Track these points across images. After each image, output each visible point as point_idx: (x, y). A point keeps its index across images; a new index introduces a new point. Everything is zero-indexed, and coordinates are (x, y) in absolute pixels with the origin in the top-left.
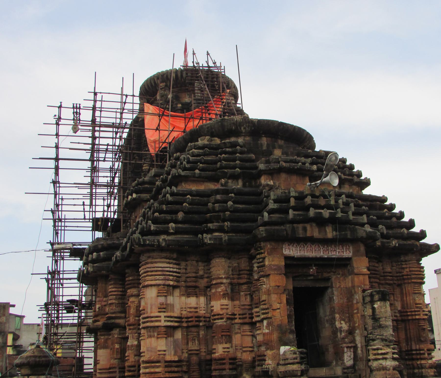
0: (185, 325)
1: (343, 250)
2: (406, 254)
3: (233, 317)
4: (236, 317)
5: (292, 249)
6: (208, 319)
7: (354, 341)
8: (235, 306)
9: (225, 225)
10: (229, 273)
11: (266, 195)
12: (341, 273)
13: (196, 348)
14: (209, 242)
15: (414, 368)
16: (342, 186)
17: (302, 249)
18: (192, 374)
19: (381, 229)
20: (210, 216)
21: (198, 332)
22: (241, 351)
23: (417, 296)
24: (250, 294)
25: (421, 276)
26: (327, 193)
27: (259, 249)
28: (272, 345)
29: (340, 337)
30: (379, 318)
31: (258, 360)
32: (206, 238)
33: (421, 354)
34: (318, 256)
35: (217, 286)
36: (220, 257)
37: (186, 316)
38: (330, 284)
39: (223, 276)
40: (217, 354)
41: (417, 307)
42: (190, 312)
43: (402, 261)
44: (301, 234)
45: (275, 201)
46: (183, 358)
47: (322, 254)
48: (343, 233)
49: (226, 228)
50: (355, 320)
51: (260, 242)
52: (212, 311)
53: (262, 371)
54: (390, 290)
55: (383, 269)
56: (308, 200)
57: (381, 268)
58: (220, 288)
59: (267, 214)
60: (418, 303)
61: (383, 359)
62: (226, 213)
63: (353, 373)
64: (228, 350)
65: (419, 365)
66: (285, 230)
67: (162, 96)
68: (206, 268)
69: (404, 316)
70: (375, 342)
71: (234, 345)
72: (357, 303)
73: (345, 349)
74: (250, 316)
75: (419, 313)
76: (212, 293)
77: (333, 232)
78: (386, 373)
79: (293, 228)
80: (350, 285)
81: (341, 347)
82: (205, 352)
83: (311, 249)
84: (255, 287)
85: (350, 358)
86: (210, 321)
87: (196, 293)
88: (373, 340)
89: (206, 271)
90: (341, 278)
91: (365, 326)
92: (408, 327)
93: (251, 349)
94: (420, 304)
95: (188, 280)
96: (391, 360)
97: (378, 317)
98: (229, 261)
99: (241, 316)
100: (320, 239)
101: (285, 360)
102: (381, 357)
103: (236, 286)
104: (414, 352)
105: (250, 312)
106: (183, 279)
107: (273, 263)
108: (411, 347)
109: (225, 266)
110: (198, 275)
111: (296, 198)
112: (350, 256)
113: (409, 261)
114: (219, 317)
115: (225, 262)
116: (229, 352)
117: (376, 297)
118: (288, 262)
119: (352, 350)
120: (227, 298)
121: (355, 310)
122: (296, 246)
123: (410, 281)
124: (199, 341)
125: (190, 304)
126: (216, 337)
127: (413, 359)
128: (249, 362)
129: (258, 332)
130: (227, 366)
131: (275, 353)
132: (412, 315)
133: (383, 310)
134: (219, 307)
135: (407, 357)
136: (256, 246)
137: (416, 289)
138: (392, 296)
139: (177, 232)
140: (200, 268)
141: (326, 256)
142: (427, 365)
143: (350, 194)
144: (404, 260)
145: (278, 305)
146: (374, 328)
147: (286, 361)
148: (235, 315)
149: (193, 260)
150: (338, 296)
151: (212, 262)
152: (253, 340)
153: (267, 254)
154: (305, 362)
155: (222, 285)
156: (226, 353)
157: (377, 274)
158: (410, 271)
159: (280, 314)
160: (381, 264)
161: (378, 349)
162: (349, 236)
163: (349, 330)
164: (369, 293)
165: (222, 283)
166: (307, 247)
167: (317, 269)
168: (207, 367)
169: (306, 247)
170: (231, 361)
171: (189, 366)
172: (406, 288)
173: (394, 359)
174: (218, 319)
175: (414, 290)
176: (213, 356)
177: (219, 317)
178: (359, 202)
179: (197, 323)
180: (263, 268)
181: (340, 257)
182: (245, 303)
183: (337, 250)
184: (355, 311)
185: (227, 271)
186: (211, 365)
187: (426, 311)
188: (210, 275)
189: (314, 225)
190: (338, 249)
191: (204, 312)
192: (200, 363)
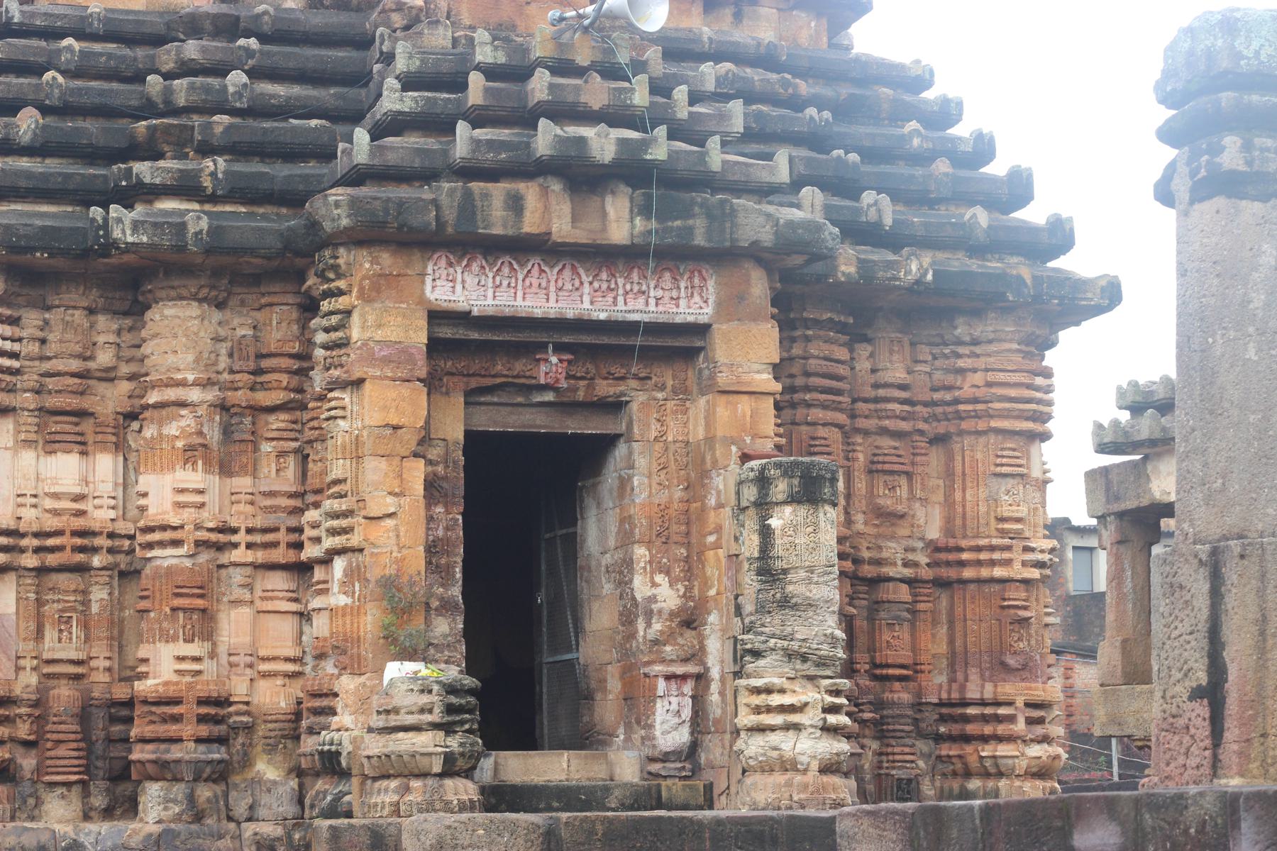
0: (30, 561)
1: (675, 294)
2: (976, 313)
3: (222, 538)
4: (235, 538)
5: (463, 282)
6: (127, 543)
7: (697, 655)
8: (234, 498)
9: (201, 170)
10: (215, 364)
11: (384, 49)
12: (670, 383)
13: (73, 655)
14: (130, 239)
15: (968, 774)
16: (747, 9)
17: (505, 283)
18: (52, 753)
19: (869, 206)
20: (148, 127)
21: (85, 592)
22: (248, 671)
23: (1009, 486)
24: (296, 451)
25: (1046, 409)
26: (623, 58)
27: (332, 275)
28: (359, 655)
29: (644, 637)
30: (785, 571)
31: (308, 709)
32: (119, 220)
33: (998, 719)
34: (570, 314)
35: (164, 412)
36: (182, 298)
37: (35, 528)
38: (624, 425)
39: (191, 377)
40: (150, 682)
41: (1003, 533)
42: (56, 513)
43: (960, 343)
44: (497, 222)
45: (409, 83)
46: (18, 691)
47: (587, 305)
48: (678, 223)
49: (207, 183)
50: (709, 571)
51: (336, 246)
52: (143, 509)
53: (321, 753)
54: (899, 456)
55: (874, 371)
56: (540, 86)
57: (867, 365)
58: (174, 424)
59: (367, 137)
60: (1006, 514)
61: (788, 727)
62: (216, 118)
63: (685, 778)
64: (196, 667)
65: (988, 763)
66: (435, 202)
68: (128, 338)
69: (948, 564)
70: (762, 662)
71: (222, 650)
72: (720, 506)
73: (661, 685)
74: (293, 537)
75: (1006, 555)
76: (145, 439)
77: (632, 220)
78: (789, 784)
79: (468, 195)
80: (701, 434)
81: (646, 675)
82: (109, 670)
83: (544, 284)
84: (315, 423)
85: (677, 720)
86: (131, 551)
87: (79, 439)
88: (757, 654)
89: (127, 353)
90: (670, 404)
91: (736, 597)
92: (958, 610)
93: (291, 667)
94: (1019, 520)
95: (51, 383)
96: (819, 733)
97: (779, 565)
98: (217, 316)
99: (258, 538)
100: (576, 244)
101: (388, 712)
102: (778, 719)
103: (242, 415)
104: (971, 711)
105: (292, 522)
106: (30, 379)
107: (379, 335)
108: (963, 688)
109: (202, 334)
110: (92, 365)
111: (491, 73)
112: (703, 319)
113: (990, 342)
114: (168, 535)
115: (202, 318)
116: (199, 672)
117: (780, 489)
118: (446, 332)
119: (688, 688)
120: (200, 462)
121: (711, 534)
122: (483, 267)
123: (981, 425)
124: (86, 626)
125: (55, 480)
126: (152, 614)
127: (967, 739)
128: (281, 717)
129: (316, 603)
130: (188, 729)
131: (364, 685)
132: (979, 563)
133: (801, 540)
134: (170, 498)
135: (942, 729)
136: (320, 261)
137: (1005, 461)
138: (903, 481)
140: (101, 339)
141: (603, 316)
142: (1022, 765)
143: (762, 50)
144: (967, 339)
145: (390, 499)
146: (761, 609)
147: (392, 717)
148: (235, 531)
149: (75, 308)
150: (649, 477)
151: (149, 315)
152: (301, 633)
153: (358, 298)
154: (467, 726)
155: (184, 412)
156: (188, 679)
157: (838, 392)
158: (989, 385)
159: (398, 536)
160: (863, 350)
161: (769, 691)
162: (700, 240)
163: (682, 609)
164: (752, 470)
165: (183, 404)
166: (526, 276)
167: (569, 362)
168: (117, 729)
169: (521, 277)
170: (204, 710)
171: (40, 720)
172: (967, 453)
173: (828, 729)
174: (161, 544)
175: (999, 461)
176: (141, 687)
177: (168, 535)
178: (796, 86)
179: (80, 557)
180: (342, 352)
181: (662, 319)
182: (275, 488)
183: (652, 293)
184: (711, 539)
185: (206, 355)
186: (129, 720)
187: (1042, 551)
188: (143, 371)
189: (556, 186)
190: (656, 287)
191: (112, 514)
192: (84, 715)
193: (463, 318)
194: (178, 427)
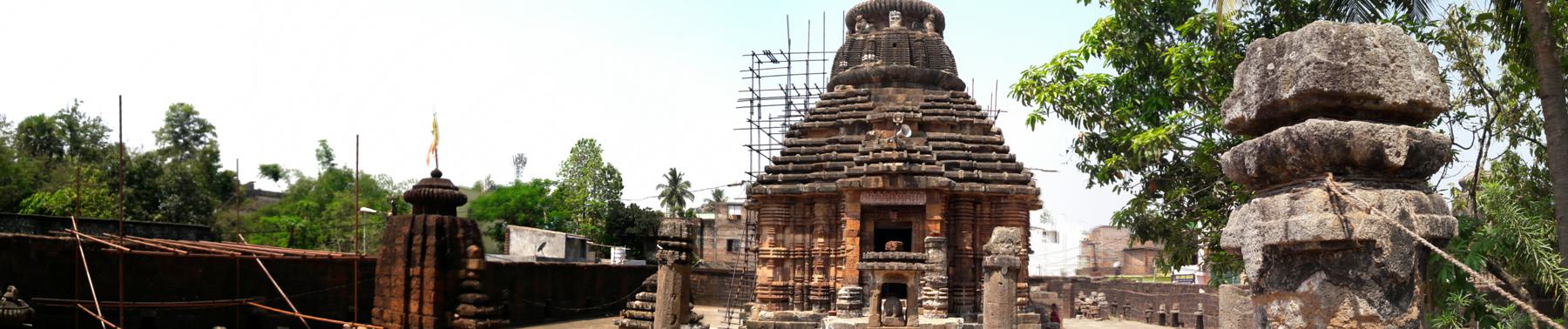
67: (859, 28)
139: (785, 182)
193: (869, 206)
194: (820, 228)
